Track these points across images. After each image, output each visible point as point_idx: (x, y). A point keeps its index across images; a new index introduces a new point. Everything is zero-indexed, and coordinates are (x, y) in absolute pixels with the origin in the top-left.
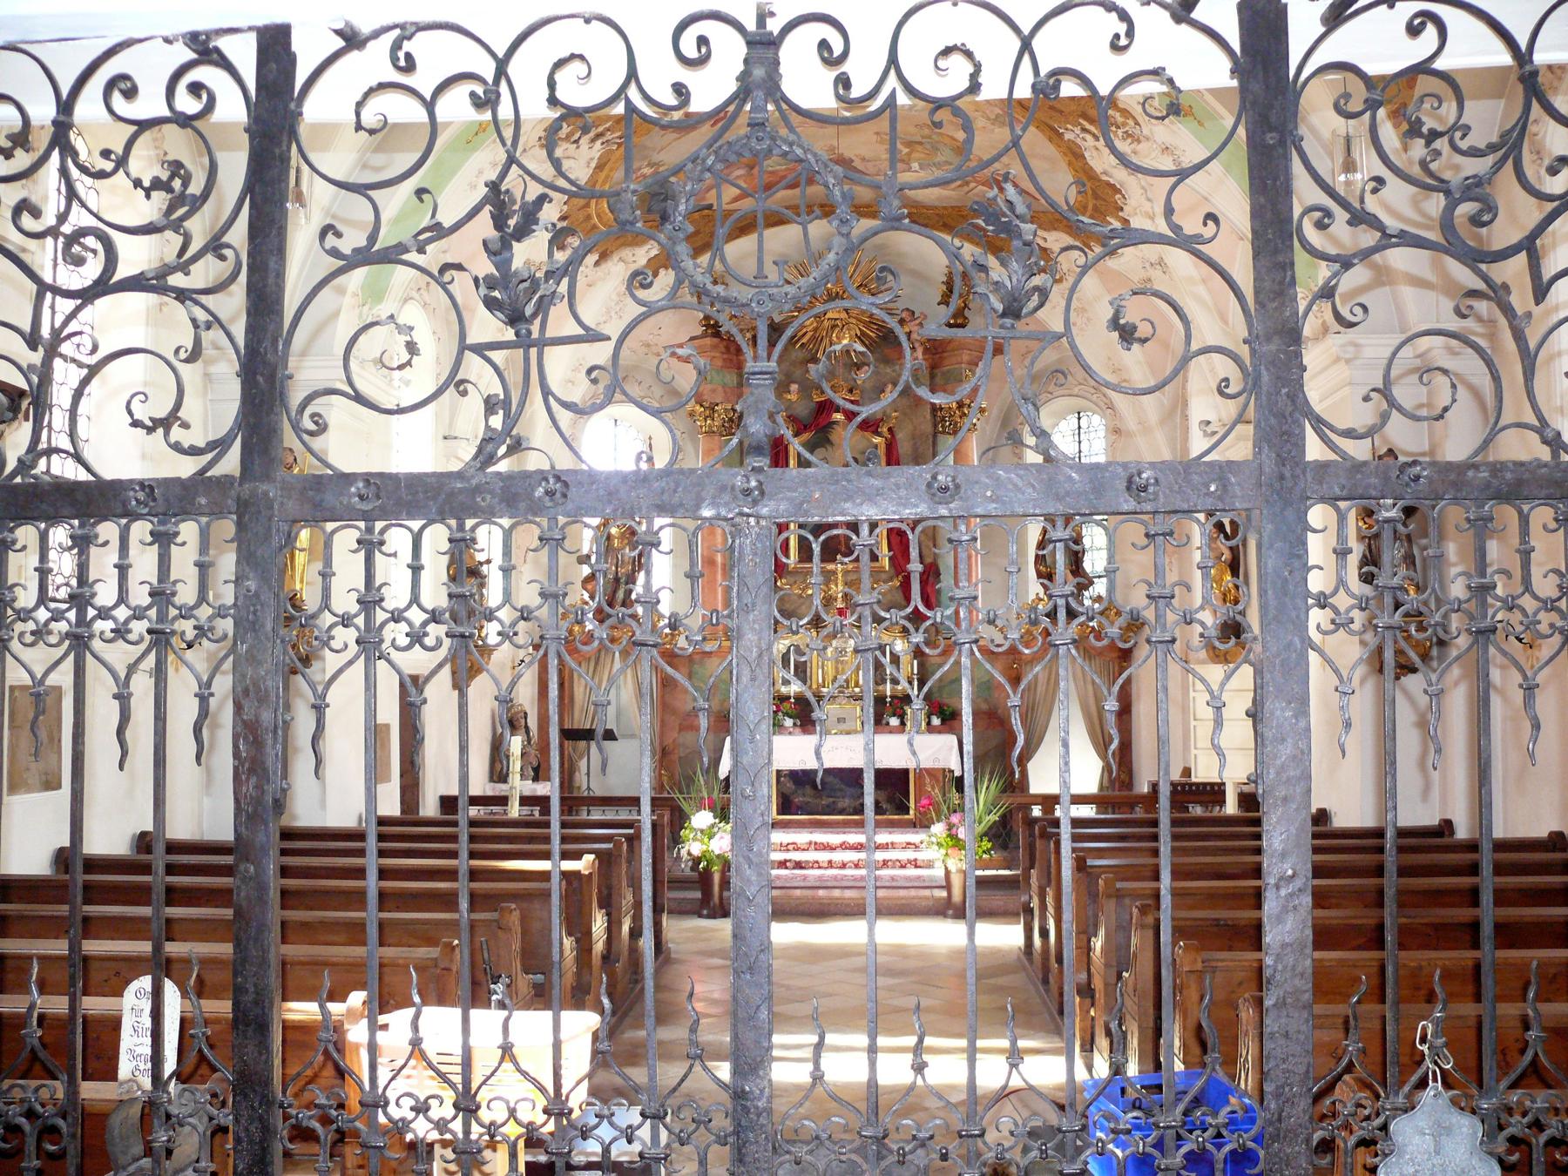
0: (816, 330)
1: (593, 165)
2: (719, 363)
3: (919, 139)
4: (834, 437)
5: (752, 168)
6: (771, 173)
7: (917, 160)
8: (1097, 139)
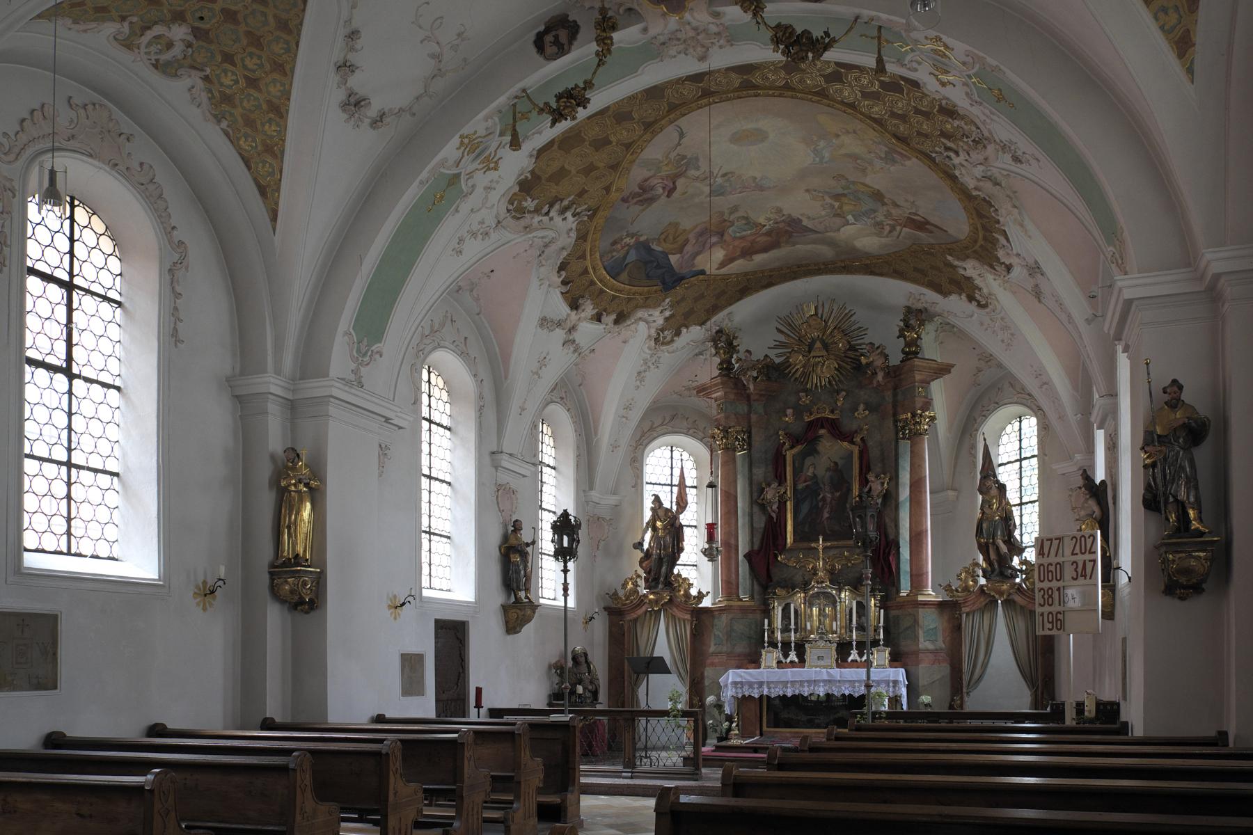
0: (804, 366)
1: (573, 235)
2: (732, 396)
3: (840, 191)
4: (820, 448)
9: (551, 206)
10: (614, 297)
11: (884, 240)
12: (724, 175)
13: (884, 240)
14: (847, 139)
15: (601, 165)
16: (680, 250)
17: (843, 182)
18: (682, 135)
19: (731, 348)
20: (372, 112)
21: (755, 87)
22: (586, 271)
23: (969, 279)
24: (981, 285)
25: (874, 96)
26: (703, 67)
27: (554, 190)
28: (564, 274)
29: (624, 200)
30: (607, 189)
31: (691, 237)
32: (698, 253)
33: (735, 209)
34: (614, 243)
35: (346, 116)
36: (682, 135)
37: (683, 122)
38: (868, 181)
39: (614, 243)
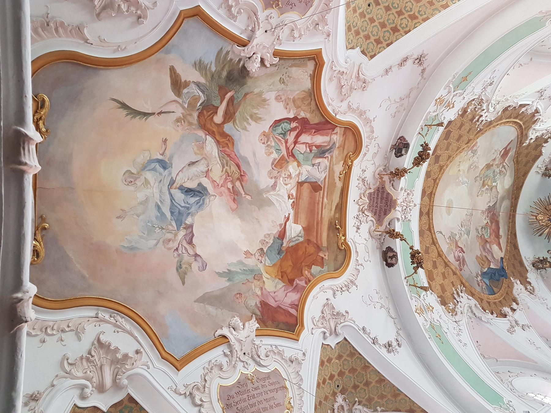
1: (470, 298)
3: (481, 182)
5: (487, 241)
6: (490, 235)
7: (492, 183)
8: (481, 116)
9: (455, 299)
10: (504, 298)
11: (508, 174)
12: (462, 226)
13: (508, 174)
14: (461, 168)
15: (443, 270)
16: (489, 262)
17: (478, 179)
18: (441, 233)
19: (543, 261)
20: (394, 344)
21: (431, 193)
22: (489, 303)
23: (537, 138)
24: (541, 133)
25: (449, 145)
26: (418, 207)
27: (448, 294)
28: (487, 311)
29: (461, 270)
30: (455, 274)
31: (484, 254)
32: (492, 254)
33: (477, 230)
34: (479, 285)
35: (392, 353)
36: (441, 233)
37: (436, 229)
38: (481, 168)
39: (479, 285)
